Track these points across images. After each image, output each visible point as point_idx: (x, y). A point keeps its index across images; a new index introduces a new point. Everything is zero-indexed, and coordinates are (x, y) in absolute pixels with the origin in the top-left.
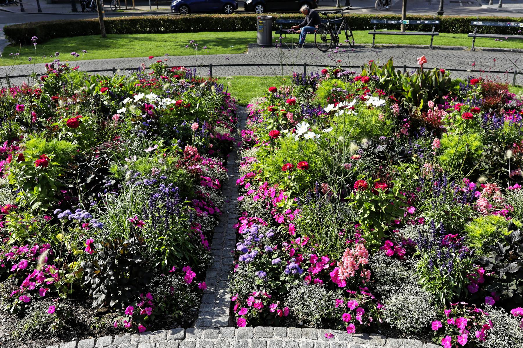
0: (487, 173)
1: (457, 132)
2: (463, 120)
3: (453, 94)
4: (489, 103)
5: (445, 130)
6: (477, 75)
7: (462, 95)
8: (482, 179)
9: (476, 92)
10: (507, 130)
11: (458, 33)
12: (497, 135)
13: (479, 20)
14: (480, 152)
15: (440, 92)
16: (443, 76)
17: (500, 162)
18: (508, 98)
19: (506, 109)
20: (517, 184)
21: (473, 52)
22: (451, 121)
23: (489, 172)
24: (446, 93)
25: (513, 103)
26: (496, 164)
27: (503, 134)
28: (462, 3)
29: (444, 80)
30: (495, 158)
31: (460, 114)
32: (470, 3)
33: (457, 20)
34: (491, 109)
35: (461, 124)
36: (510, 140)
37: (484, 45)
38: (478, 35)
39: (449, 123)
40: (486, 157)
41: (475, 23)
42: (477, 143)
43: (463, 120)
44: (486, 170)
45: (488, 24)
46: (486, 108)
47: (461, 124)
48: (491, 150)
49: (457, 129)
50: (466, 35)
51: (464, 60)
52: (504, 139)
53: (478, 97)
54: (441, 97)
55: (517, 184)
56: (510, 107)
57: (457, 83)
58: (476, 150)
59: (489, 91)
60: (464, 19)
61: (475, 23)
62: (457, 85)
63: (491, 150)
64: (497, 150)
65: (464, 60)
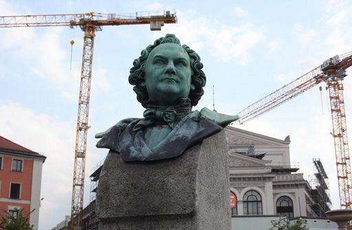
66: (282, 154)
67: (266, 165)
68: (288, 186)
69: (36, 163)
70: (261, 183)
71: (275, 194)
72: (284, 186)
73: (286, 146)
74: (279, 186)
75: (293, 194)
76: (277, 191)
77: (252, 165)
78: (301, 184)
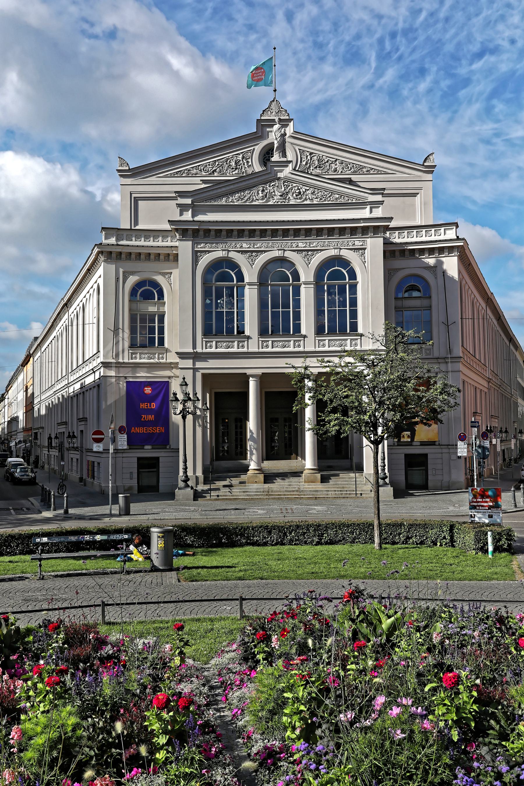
0: (93, 762)
1: (42, 709)
2: (48, 688)
3: (25, 649)
4: (78, 655)
5: (24, 711)
6: (54, 617)
7: (38, 649)
8: (89, 774)
9: (57, 642)
10: (108, 691)
11: (15, 554)
12: (97, 701)
13: (44, 535)
14: (79, 732)
15: (6, 651)
16: (7, 625)
17: (107, 741)
18: (102, 642)
19: (103, 660)
20: (135, 769)
21: (42, 581)
22: (31, 693)
23: (97, 760)
24: (14, 651)
25: (108, 650)
26: (103, 745)
27: (104, 698)
28: (14, 509)
29: (9, 631)
30: (101, 737)
31: (42, 681)
32: (25, 509)
33: (12, 537)
34: (81, 664)
35: (45, 696)
36: (114, 704)
37: (55, 568)
38: (44, 556)
39: (28, 698)
40: (89, 738)
41: (38, 540)
42: (73, 720)
43: (48, 688)
44: (91, 758)
45: (56, 540)
46: (75, 662)
47: (45, 696)
48: (94, 725)
49: (42, 705)
50: (28, 557)
51: (30, 594)
52: (106, 705)
53: (61, 650)
54: (7, 658)
55: (135, 769)
56: (105, 655)
57: (29, 631)
58: (74, 730)
59: (76, 637)
60: (21, 534)
61: (38, 540)
62: (29, 636)
63: (94, 725)
64: (101, 723)
65: (30, 594)
77: (342, 201)
78: (451, 249)
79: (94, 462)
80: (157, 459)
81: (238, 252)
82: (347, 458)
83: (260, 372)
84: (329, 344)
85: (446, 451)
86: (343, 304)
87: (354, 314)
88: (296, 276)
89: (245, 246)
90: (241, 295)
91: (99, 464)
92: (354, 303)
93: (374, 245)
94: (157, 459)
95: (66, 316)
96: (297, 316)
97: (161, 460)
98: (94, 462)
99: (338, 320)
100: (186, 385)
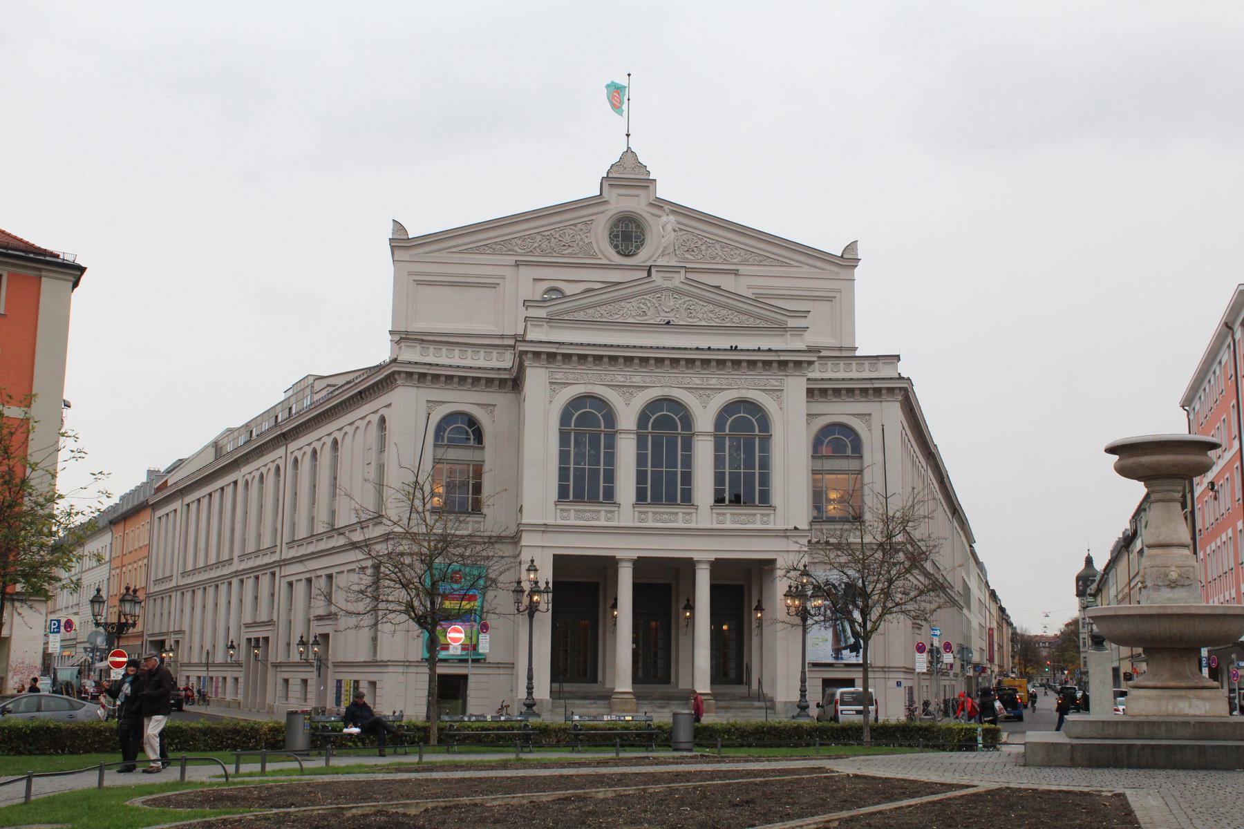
66: (829, 299)
67: (792, 323)
68: (850, 391)
69: (50, 286)
70: (771, 379)
71: (811, 416)
72: (837, 392)
73: (844, 273)
74: (823, 392)
75: (866, 416)
76: (820, 407)
77: (751, 322)
78: (890, 390)
79: (357, 682)
80: (465, 678)
81: (608, 386)
82: (739, 680)
83: (635, 555)
84: (731, 518)
85: (882, 675)
86: (749, 464)
87: (765, 479)
88: (687, 421)
89: (620, 379)
90: (611, 445)
91: (373, 684)
92: (765, 464)
93: (795, 386)
94: (465, 678)
95: (280, 452)
96: (687, 478)
97: (471, 679)
98: (357, 682)
99: (744, 488)
100: (536, 570)
